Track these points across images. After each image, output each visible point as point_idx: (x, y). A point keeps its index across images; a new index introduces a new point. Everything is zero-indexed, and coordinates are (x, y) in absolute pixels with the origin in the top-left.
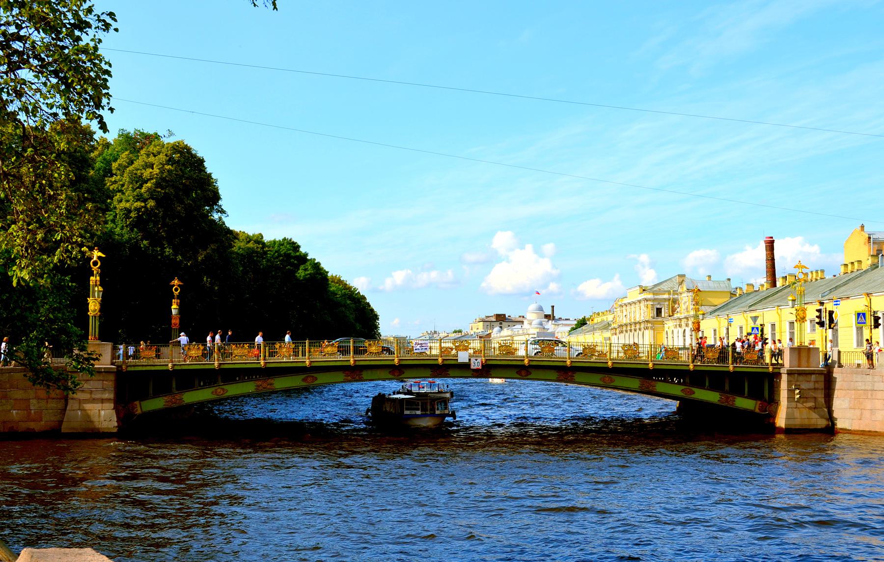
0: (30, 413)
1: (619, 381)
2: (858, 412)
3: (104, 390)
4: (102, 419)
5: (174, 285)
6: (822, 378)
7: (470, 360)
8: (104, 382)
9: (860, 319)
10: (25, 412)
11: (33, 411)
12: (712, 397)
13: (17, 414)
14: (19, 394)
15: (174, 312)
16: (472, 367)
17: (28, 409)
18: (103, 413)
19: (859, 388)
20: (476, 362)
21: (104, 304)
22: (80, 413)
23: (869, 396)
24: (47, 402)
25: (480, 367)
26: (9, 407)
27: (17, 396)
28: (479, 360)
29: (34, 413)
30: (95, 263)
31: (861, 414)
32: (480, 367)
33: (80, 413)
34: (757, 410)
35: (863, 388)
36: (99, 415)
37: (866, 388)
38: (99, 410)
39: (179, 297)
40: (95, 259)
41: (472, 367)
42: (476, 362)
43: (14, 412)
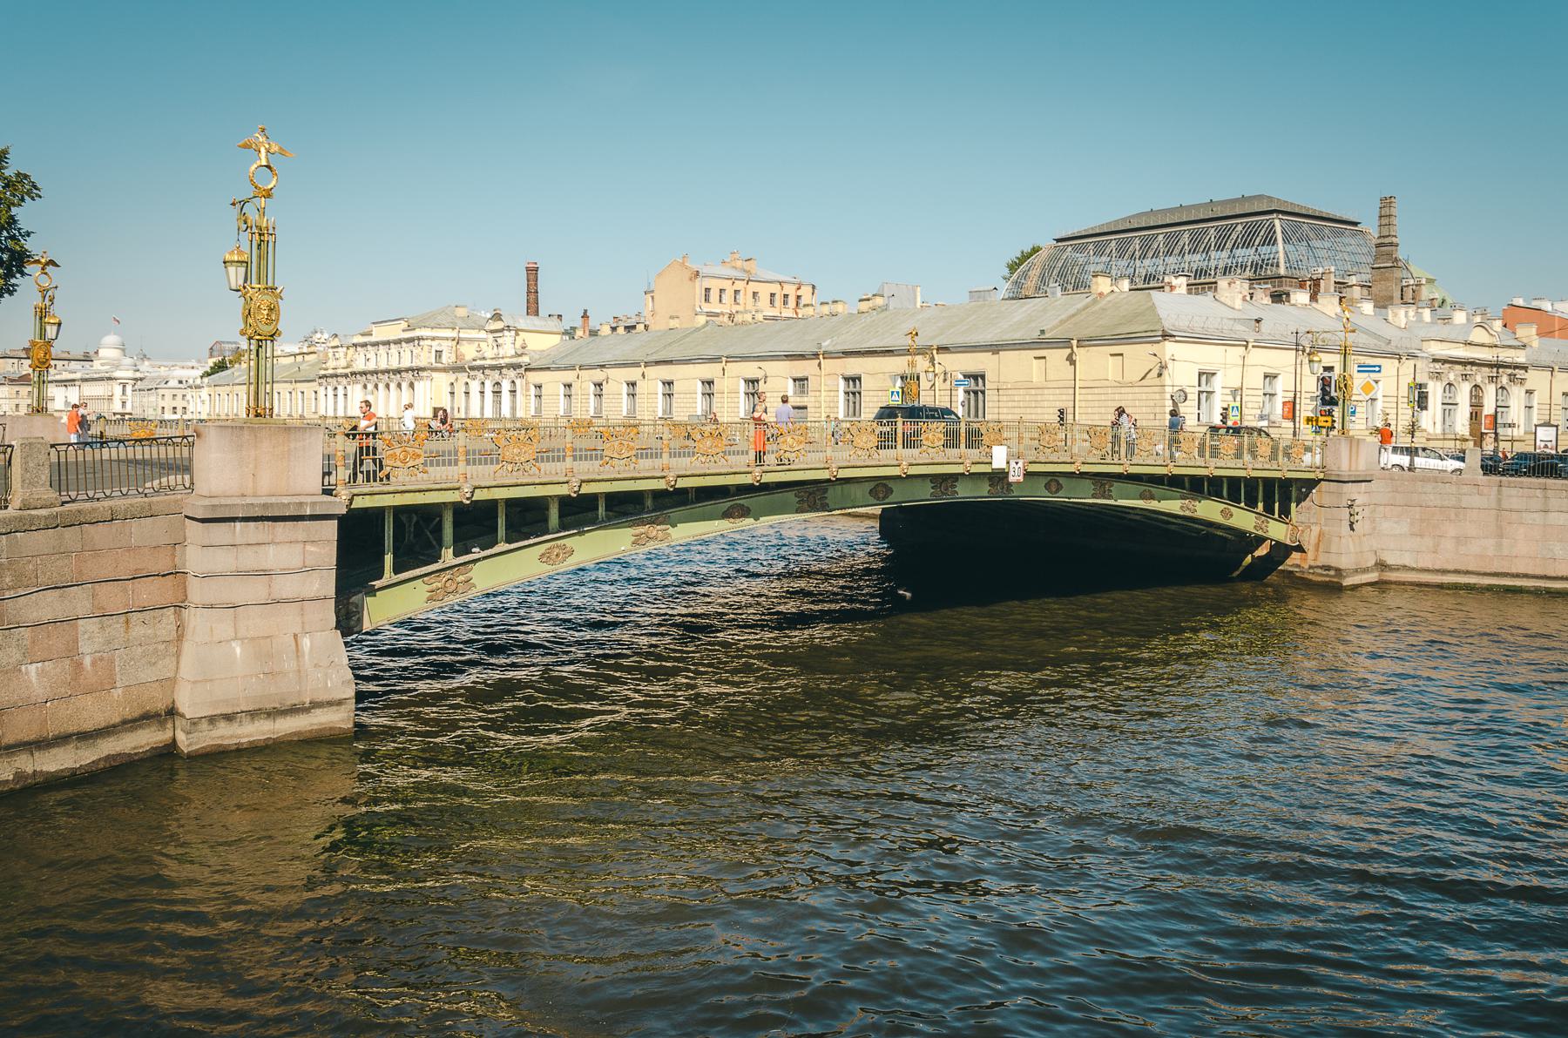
0: (79, 666)
7: (1008, 463)
8: (309, 548)
10: (68, 662)
11: (87, 661)
12: (1243, 519)
16: (1011, 479)
17: (72, 653)
18: (306, 642)
19: (1431, 504)
20: (1017, 467)
22: (238, 650)
23: (1453, 516)
24: (127, 622)
26: (16, 655)
27: (33, 615)
29: (94, 663)
33: (238, 650)
34: (1288, 542)
35: (1438, 503)
37: (1446, 503)
38: (295, 636)
42: (1017, 467)
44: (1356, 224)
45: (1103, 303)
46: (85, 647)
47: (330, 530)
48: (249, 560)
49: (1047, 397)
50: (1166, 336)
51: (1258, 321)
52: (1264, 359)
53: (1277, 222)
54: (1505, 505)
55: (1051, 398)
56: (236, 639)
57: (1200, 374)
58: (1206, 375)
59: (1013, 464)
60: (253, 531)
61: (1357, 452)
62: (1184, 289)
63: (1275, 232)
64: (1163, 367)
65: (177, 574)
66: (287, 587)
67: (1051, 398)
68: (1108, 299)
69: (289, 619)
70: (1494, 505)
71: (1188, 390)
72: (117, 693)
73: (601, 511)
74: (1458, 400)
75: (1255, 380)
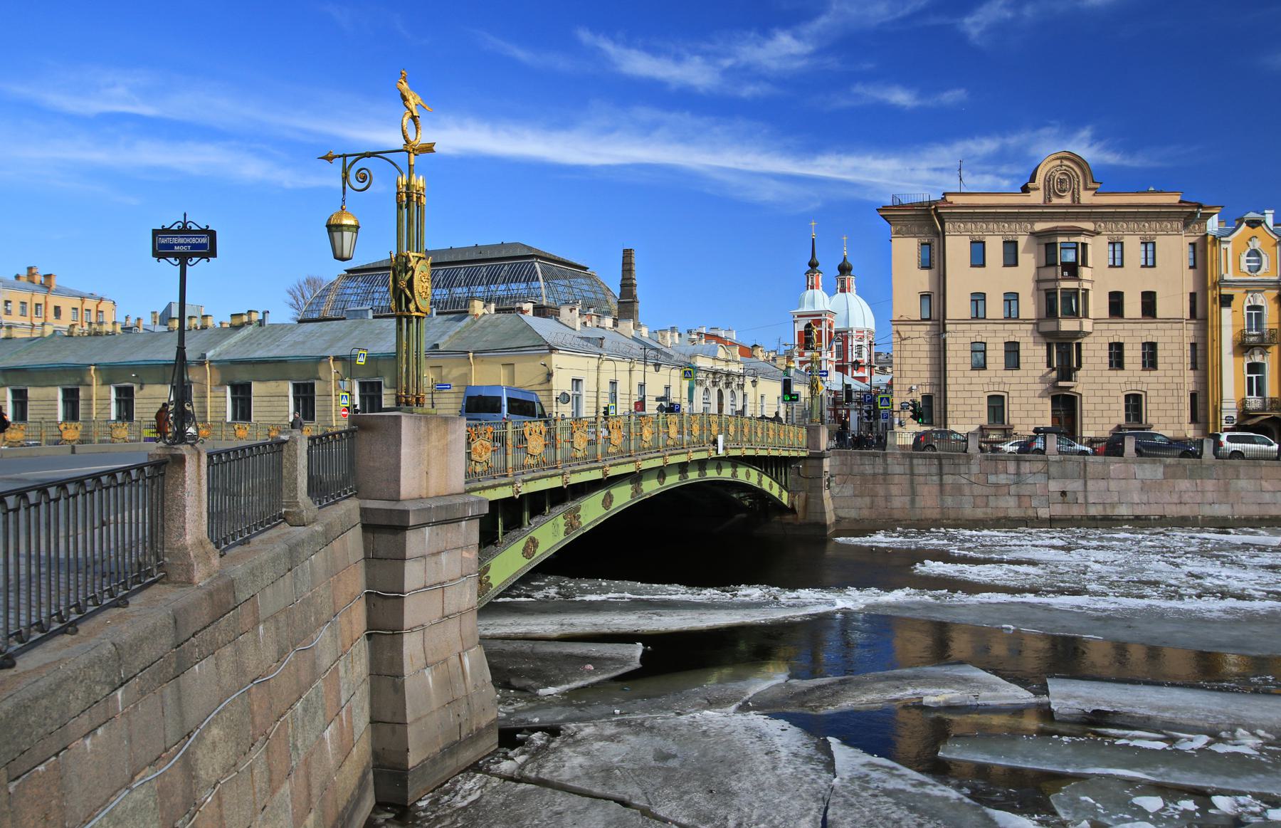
2: (867, 500)
31: (872, 502)
44: (585, 269)
45: (480, 322)
49: (444, 401)
50: (552, 350)
51: (602, 339)
52: (611, 369)
53: (536, 264)
54: (916, 471)
55: (447, 401)
56: (427, 666)
57: (573, 380)
58: (577, 382)
62: (531, 313)
63: (536, 272)
64: (550, 375)
67: (447, 401)
68: (483, 319)
70: (908, 472)
71: (567, 392)
74: (711, 400)
75: (606, 387)
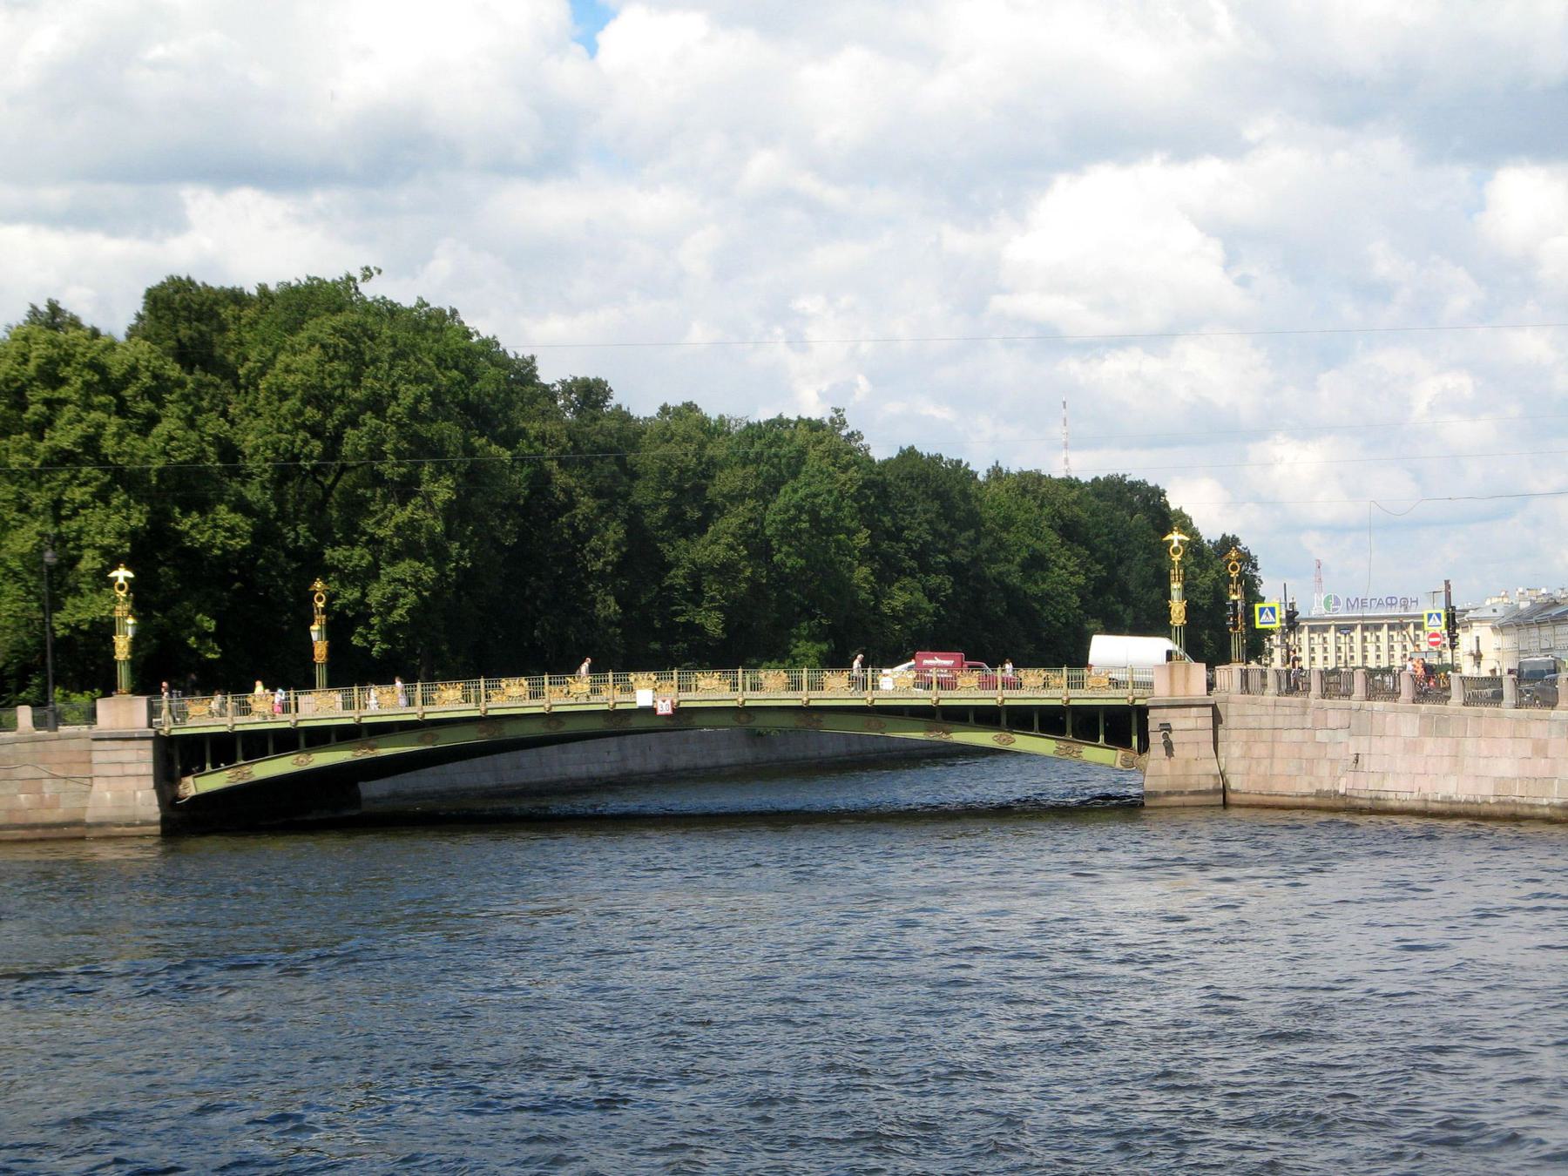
1: (597, 725)
3: (140, 762)
4: (139, 801)
5: (315, 592)
6: (1209, 711)
9: (1264, 616)
11: (47, 796)
13: (26, 799)
14: (28, 772)
15: (314, 636)
16: (659, 712)
17: (40, 792)
18: (139, 794)
21: (135, 644)
25: (670, 712)
28: (668, 702)
30: (121, 587)
32: (670, 712)
36: (135, 799)
39: (324, 611)
40: (121, 581)
41: (659, 712)
43: (22, 796)
46: (45, 790)
47: (149, 745)
48: (114, 757)
59: (660, 702)
60: (119, 744)
61: (1187, 680)
65: (90, 762)
66: (130, 769)
69: (132, 783)
72: (61, 811)
73: (333, 737)
